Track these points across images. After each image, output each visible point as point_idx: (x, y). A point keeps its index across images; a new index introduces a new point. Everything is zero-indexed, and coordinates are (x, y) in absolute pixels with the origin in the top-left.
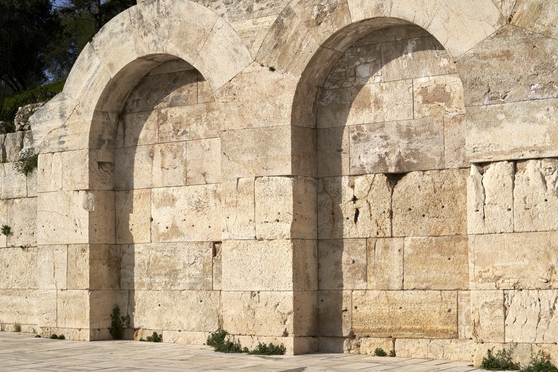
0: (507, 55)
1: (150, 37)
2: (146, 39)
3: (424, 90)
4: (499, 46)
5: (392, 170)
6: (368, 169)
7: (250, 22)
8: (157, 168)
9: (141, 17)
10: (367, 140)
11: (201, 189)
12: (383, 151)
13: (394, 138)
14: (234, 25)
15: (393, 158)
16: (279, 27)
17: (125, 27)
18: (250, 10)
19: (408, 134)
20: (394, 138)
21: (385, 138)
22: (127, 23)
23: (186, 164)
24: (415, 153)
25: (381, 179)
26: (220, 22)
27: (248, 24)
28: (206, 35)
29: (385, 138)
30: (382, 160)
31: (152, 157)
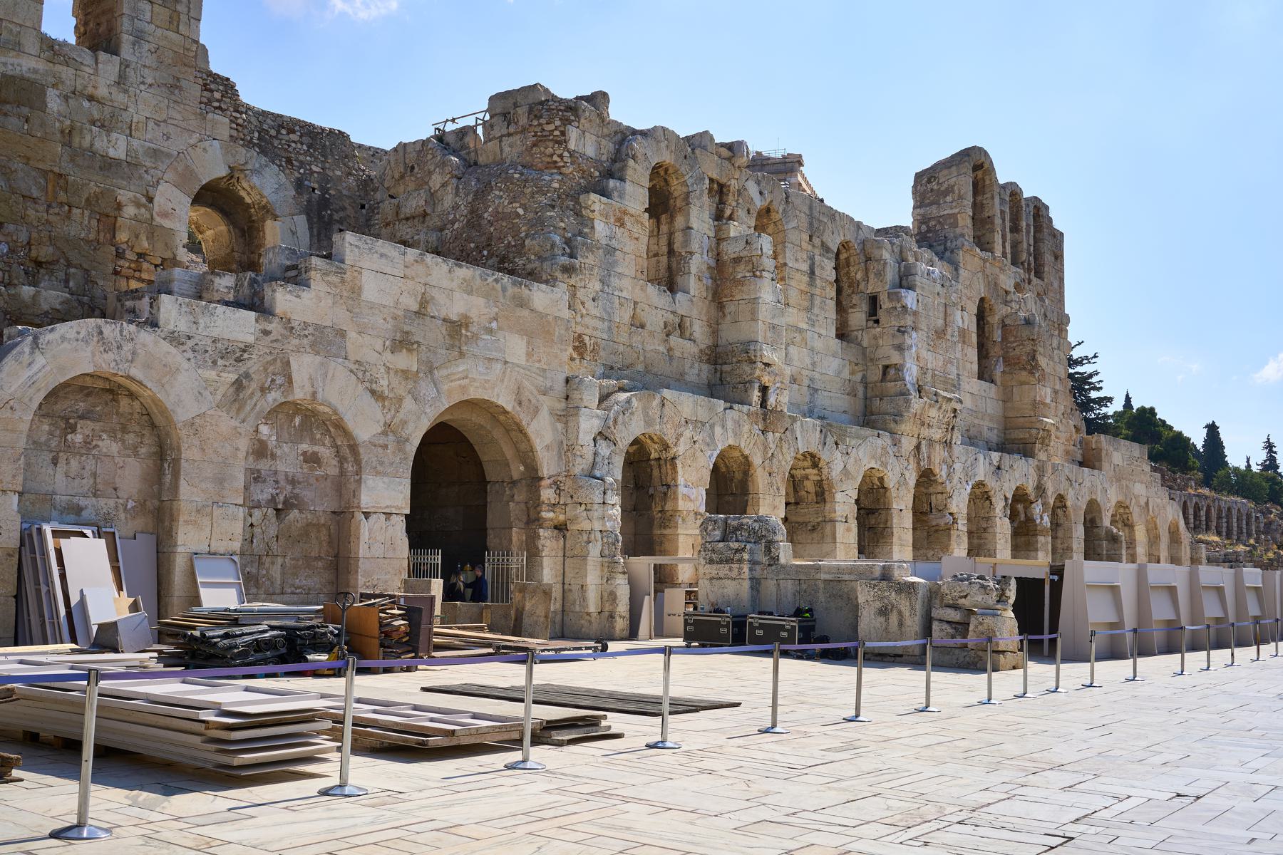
0: (385, 447)
1: (110, 356)
2: (105, 356)
3: (304, 453)
4: (382, 441)
5: (280, 506)
6: (263, 503)
7: (214, 373)
8: (60, 476)
9: (101, 333)
10: (264, 481)
11: (112, 502)
12: (274, 492)
13: (282, 483)
14: (200, 371)
15: (282, 498)
16: (238, 385)
17: (81, 336)
18: (214, 362)
19: (293, 482)
20: (282, 483)
21: (277, 482)
22: (83, 333)
23: (94, 475)
24: (296, 497)
25: (271, 511)
26: (185, 365)
27: (211, 374)
28: (173, 372)
29: (277, 482)
30: (273, 499)
31: (56, 465)
